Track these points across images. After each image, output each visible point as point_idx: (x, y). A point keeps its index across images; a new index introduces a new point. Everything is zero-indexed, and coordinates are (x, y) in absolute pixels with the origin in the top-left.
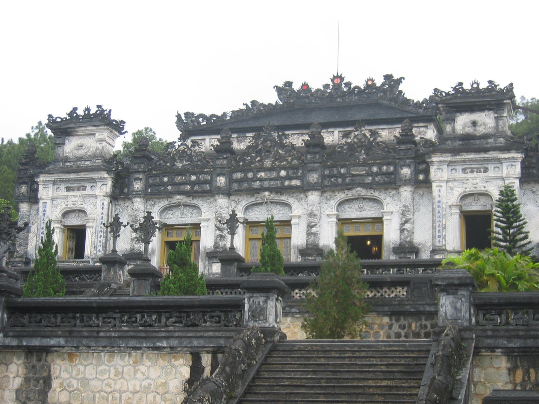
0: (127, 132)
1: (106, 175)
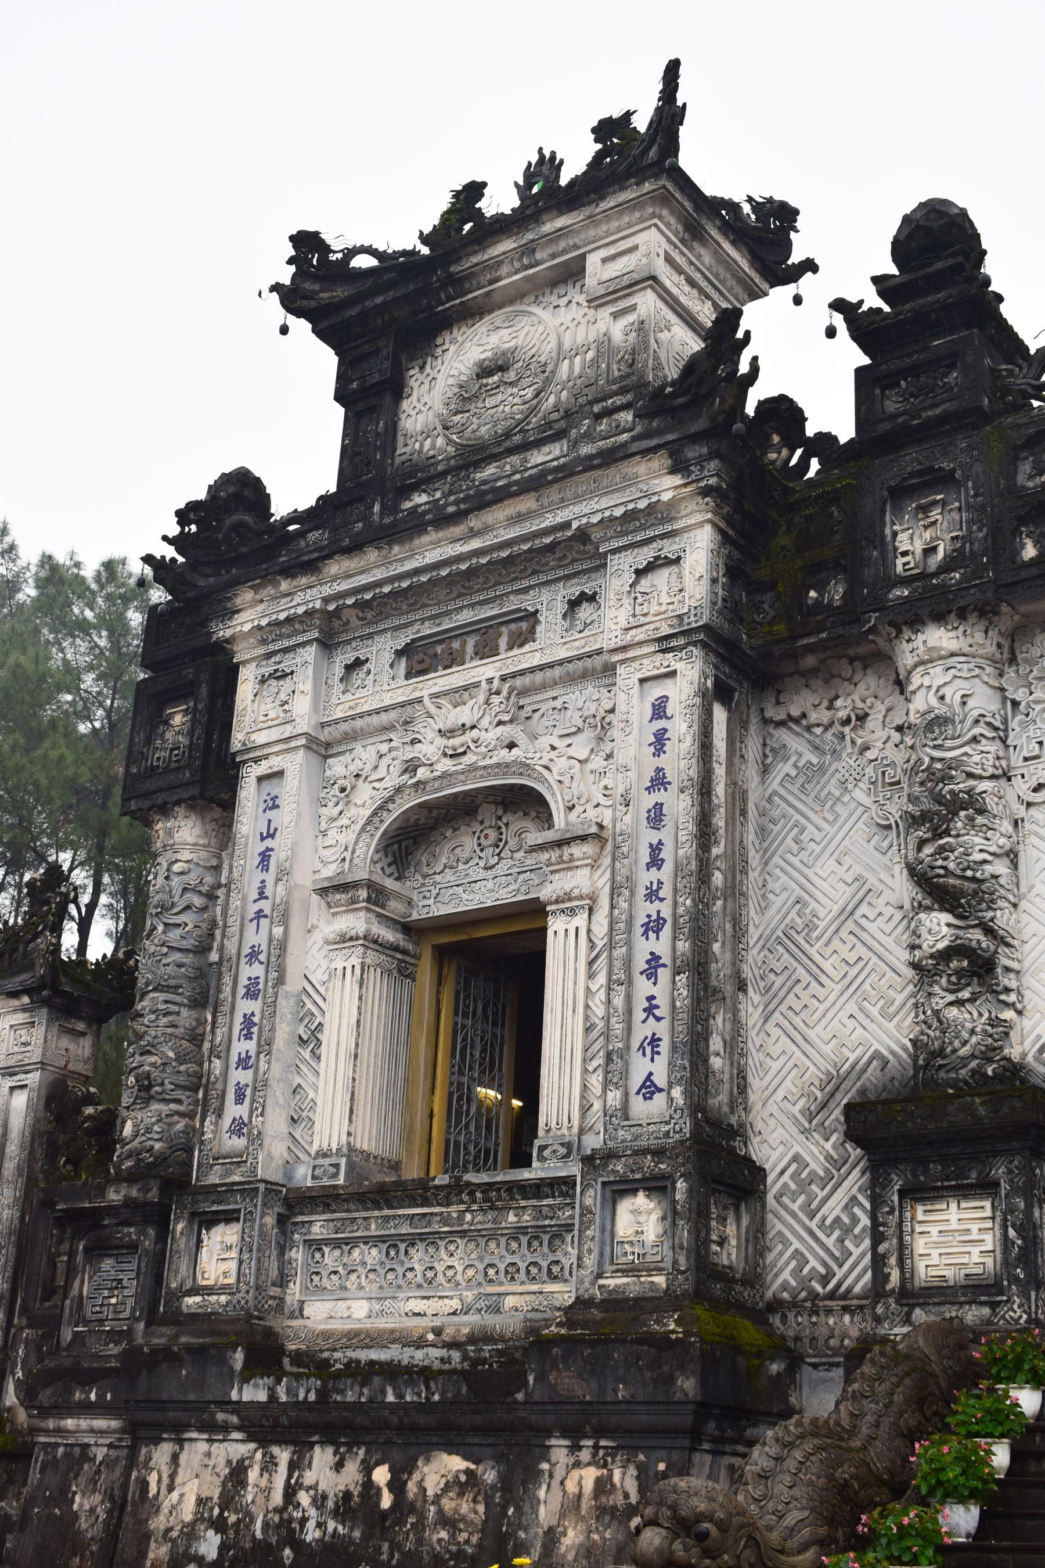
0: (810, 266)
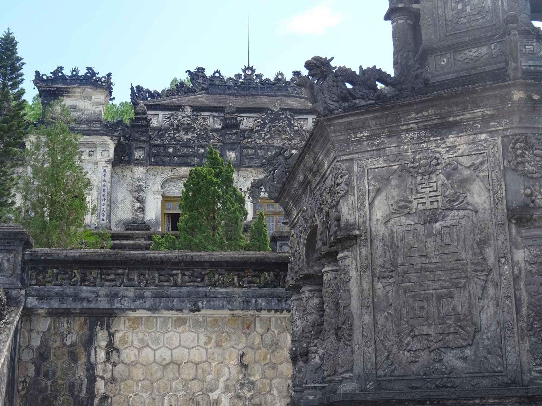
1: (110, 141)
